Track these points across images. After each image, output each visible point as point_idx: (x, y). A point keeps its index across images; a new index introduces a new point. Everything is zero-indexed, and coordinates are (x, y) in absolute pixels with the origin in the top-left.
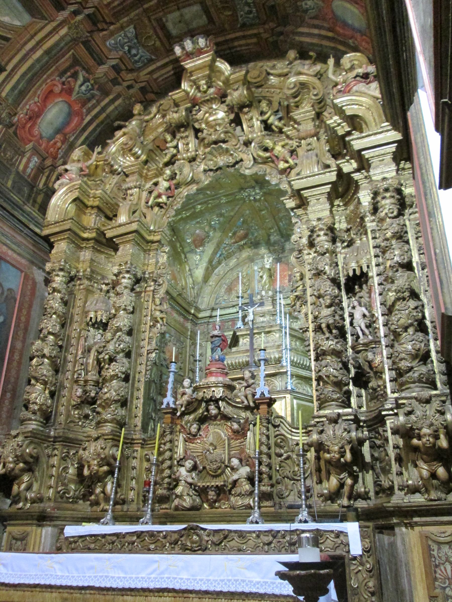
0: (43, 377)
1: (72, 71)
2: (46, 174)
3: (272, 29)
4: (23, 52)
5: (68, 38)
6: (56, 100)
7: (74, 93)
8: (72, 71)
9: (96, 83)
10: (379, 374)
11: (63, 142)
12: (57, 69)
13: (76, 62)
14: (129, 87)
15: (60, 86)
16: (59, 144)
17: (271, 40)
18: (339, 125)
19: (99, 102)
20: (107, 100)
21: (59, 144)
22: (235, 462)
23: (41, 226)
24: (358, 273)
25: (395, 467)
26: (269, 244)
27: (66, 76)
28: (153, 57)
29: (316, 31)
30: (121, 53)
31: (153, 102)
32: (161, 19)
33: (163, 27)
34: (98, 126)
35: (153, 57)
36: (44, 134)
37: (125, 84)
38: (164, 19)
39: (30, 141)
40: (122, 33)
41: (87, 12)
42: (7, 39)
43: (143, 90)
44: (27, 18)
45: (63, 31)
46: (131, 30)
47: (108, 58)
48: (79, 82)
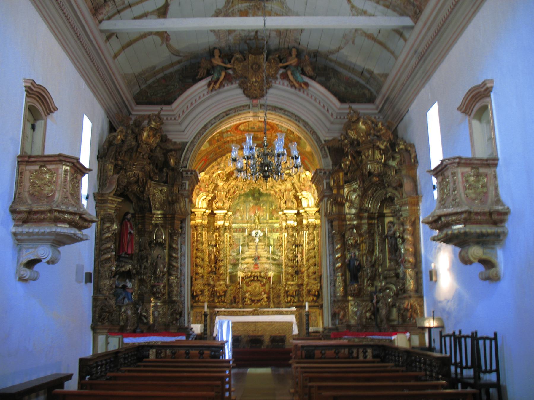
10: (303, 273)
22: (263, 293)
23: (193, 208)
25: (305, 297)
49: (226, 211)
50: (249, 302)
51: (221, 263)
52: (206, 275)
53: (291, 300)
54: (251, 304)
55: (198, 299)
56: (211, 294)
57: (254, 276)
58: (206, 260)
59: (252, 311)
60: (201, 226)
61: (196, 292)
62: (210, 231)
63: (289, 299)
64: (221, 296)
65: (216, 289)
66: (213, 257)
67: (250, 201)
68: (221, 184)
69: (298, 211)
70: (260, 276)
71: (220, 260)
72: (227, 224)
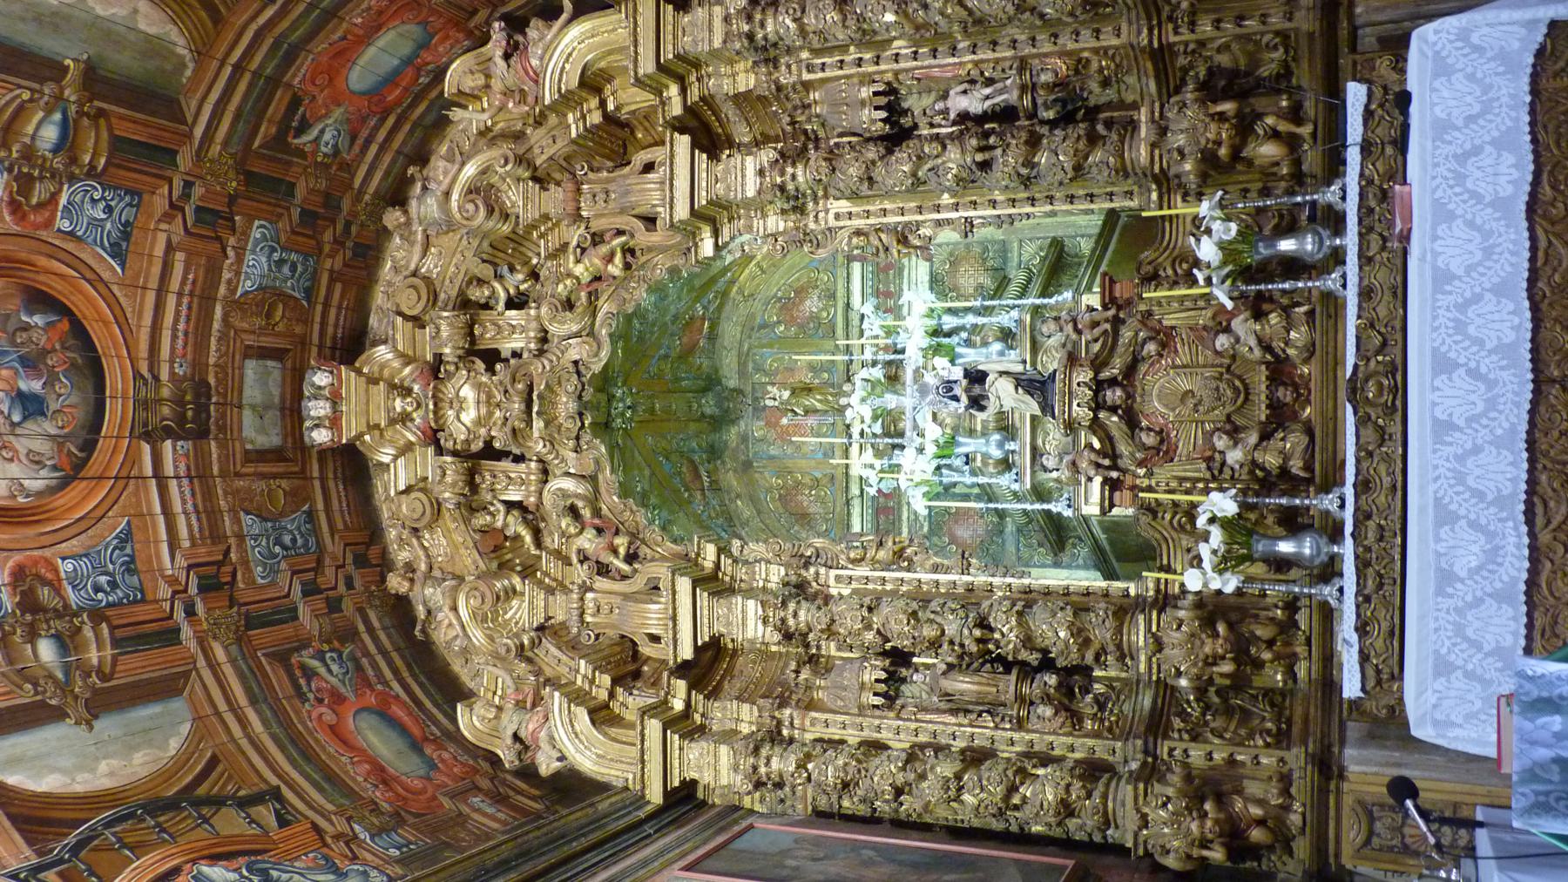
0: (1010, 773)
1: (298, 673)
2: (511, 793)
3: (336, 241)
4: (244, 743)
5: (234, 649)
6: (352, 727)
7: (343, 690)
8: (298, 673)
9: (329, 642)
11: (441, 747)
12: (288, 698)
13: (282, 657)
14: (349, 584)
15: (323, 710)
16: (446, 755)
17: (349, 254)
18: (584, 117)
19: (367, 654)
20: (366, 638)
21: (446, 755)
22: (1222, 341)
23: (641, 800)
24: (883, 101)
26: (719, 422)
27: (305, 689)
28: (305, 508)
29: (374, 149)
30: (283, 565)
31: (384, 553)
32: (247, 452)
33: (262, 455)
34: (413, 676)
35: (305, 508)
36: (422, 772)
37: (342, 588)
38: (249, 447)
39: (434, 798)
40: (250, 543)
41: (193, 590)
42: (213, 762)
43: (361, 561)
44: (178, 705)
45: (220, 654)
46: (247, 520)
47: (288, 595)
48: (322, 670)
49: (684, 585)
50: (1294, 441)
51: (1007, 632)
52: (1083, 747)
53: (1275, 135)
54: (1310, 432)
55: (1261, 822)
56: (1229, 711)
57: (1097, 405)
58: (983, 732)
59: (1362, 422)
60: (756, 750)
61: (1205, 844)
62: (809, 688)
63: (1268, 151)
64: (1241, 650)
65: (1183, 682)
66: (964, 685)
67: (744, 438)
68: (524, 611)
69: (679, 126)
70: (1098, 364)
71: (979, 641)
72: (775, 575)
